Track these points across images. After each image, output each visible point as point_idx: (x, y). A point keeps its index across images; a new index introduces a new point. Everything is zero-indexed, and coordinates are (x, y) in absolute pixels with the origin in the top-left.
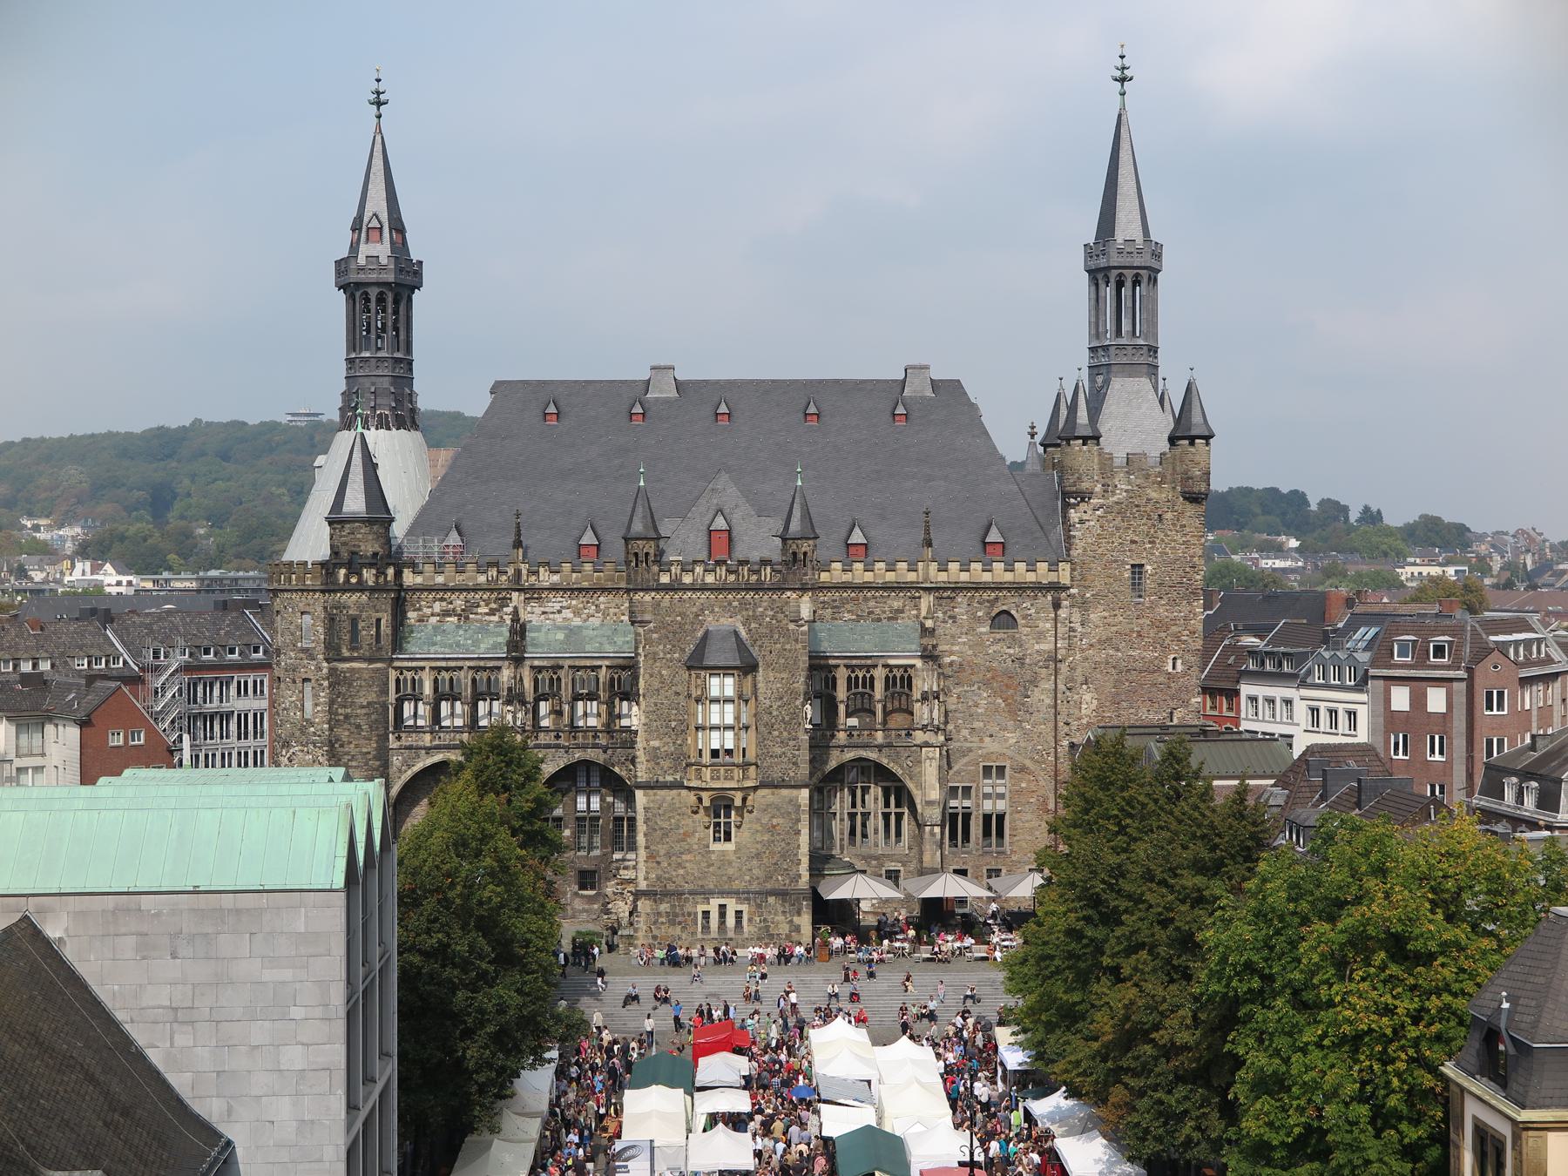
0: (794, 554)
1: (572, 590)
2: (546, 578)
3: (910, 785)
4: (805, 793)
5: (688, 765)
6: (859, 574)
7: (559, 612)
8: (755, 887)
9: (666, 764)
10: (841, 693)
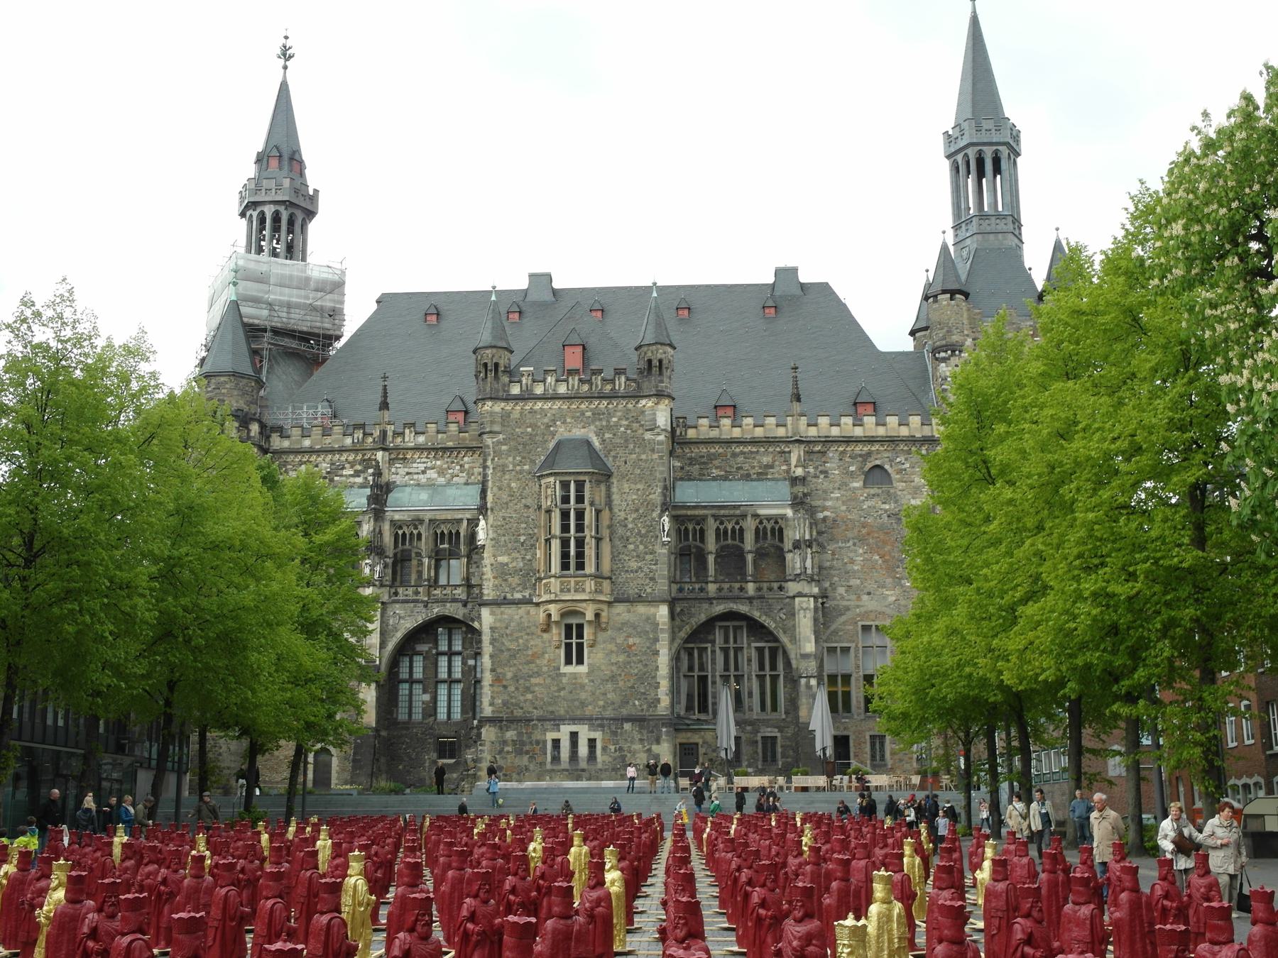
0: (650, 361)
1: (436, 450)
2: (410, 439)
3: (784, 639)
4: (663, 611)
5: (540, 579)
6: (726, 428)
7: (424, 472)
8: (609, 713)
9: (515, 581)
10: (711, 544)
